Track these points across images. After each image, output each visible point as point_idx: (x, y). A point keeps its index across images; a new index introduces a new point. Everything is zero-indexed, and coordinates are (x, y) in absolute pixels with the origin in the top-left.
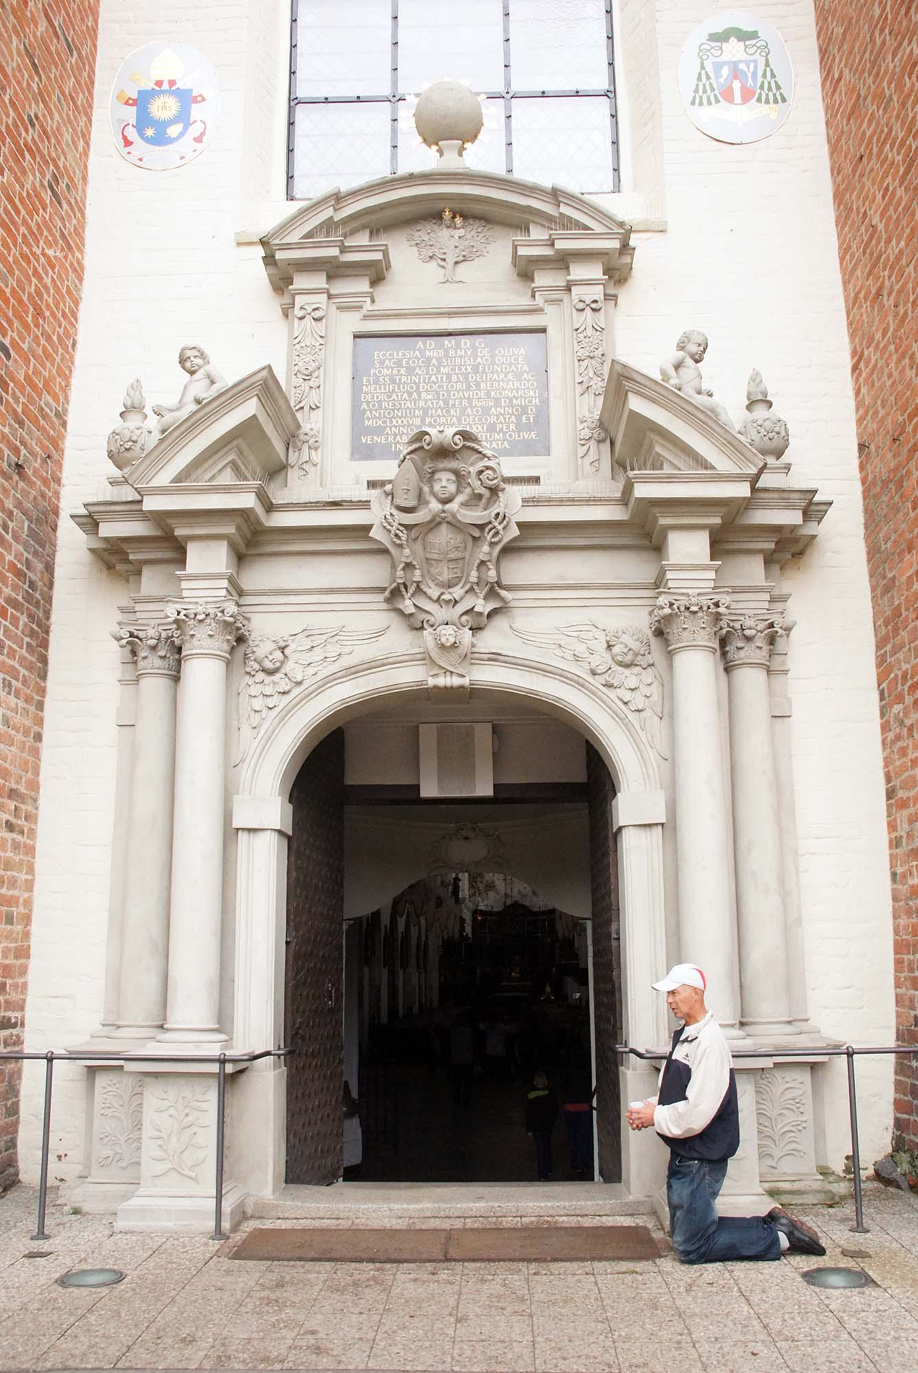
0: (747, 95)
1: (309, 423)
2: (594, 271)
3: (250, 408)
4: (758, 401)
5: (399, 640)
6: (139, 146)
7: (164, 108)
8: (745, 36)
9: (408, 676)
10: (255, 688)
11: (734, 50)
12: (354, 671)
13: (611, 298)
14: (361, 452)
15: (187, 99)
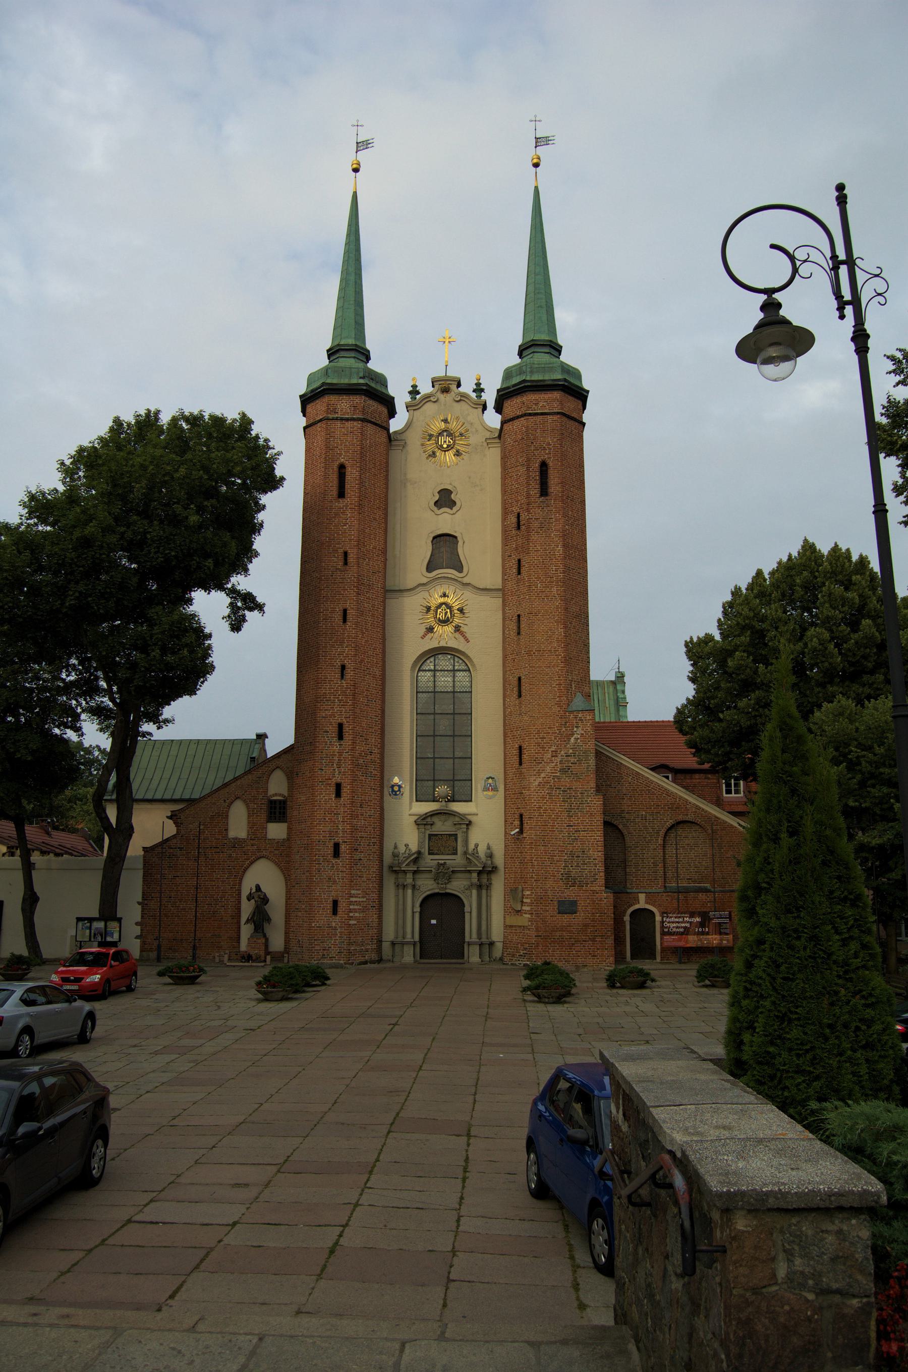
0: (492, 789)
1: (423, 851)
2: (465, 826)
3: (415, 856)
4: (489, 848)
5: (435, 885)
6: (392, 796)
7: (396, 788)
8: (492, 778)
9: (437, 891)
10: (416, 892)
11: (490, 781)
12: (429, 890)
13: (467, 829)
14: (429, 854)
15: (400, 787)
